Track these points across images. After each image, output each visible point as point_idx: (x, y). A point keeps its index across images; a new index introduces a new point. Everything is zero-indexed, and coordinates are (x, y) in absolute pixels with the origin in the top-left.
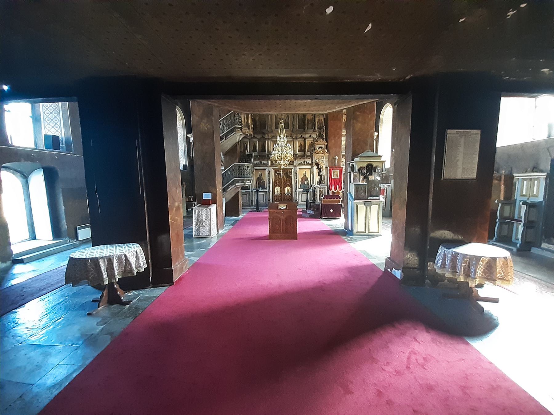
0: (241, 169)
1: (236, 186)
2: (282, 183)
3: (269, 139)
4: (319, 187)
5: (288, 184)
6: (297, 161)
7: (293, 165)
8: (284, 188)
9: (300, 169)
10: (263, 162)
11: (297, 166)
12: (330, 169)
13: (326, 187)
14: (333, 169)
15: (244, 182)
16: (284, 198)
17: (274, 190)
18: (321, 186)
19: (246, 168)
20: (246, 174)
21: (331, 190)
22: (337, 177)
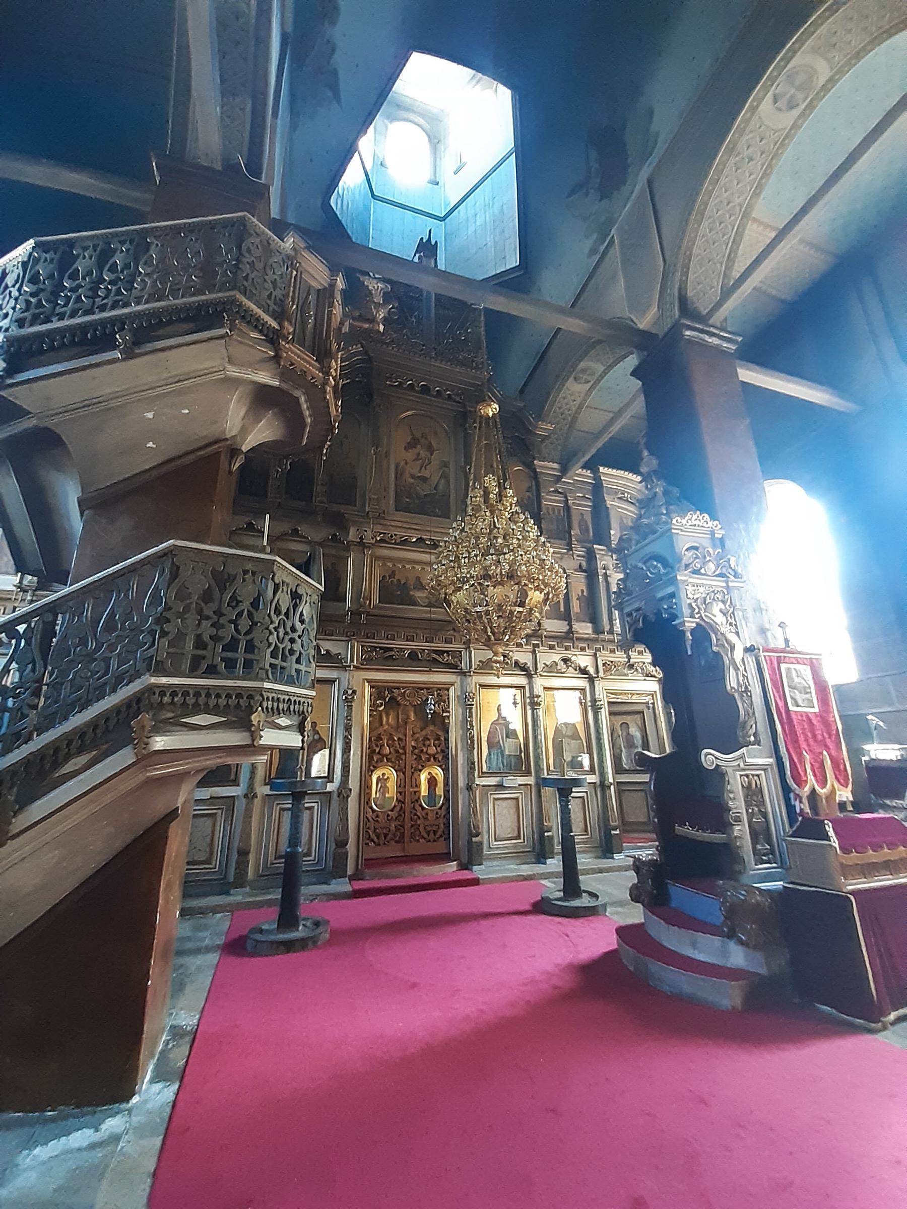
0: (235, 601)
1: (148, 758)
2: (404, 748)
5: (434, 756)
6: (472, 649)
7: (456, 667)
8: (416, 774)
9: (483, 686)
15: (244, 724)
16: (415, 826)
17: (365, 786)
19: (285, 601)
20: (274, 655)
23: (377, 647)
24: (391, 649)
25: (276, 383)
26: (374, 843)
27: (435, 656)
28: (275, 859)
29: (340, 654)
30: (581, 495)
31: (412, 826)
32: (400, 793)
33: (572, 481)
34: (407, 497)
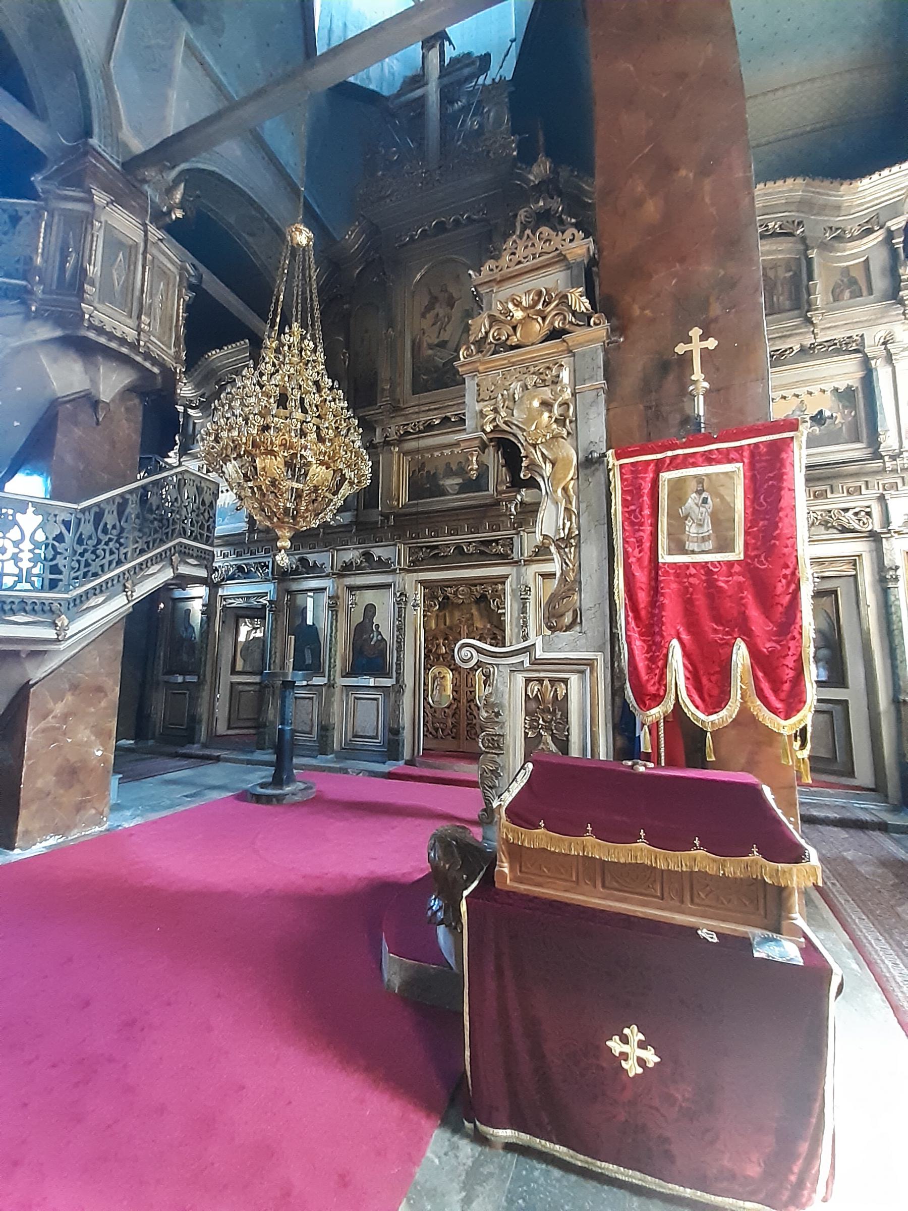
3: (387, 443)
4: (525, 659)
10: (378, 552)
11: (528, 562)
12: (632, 476)
13: (590, 663)
14: (660, 466)
18: (539, 653)
21: (658, 699)
22: (725, 545)
23: (422, 547)
24: (436, 547)
26: (433, 735)
27: (482, 548)
28: (353, 737)
29: (390, 559)
31: (468, 724)
32: (456, 692)
34: (424, 375)
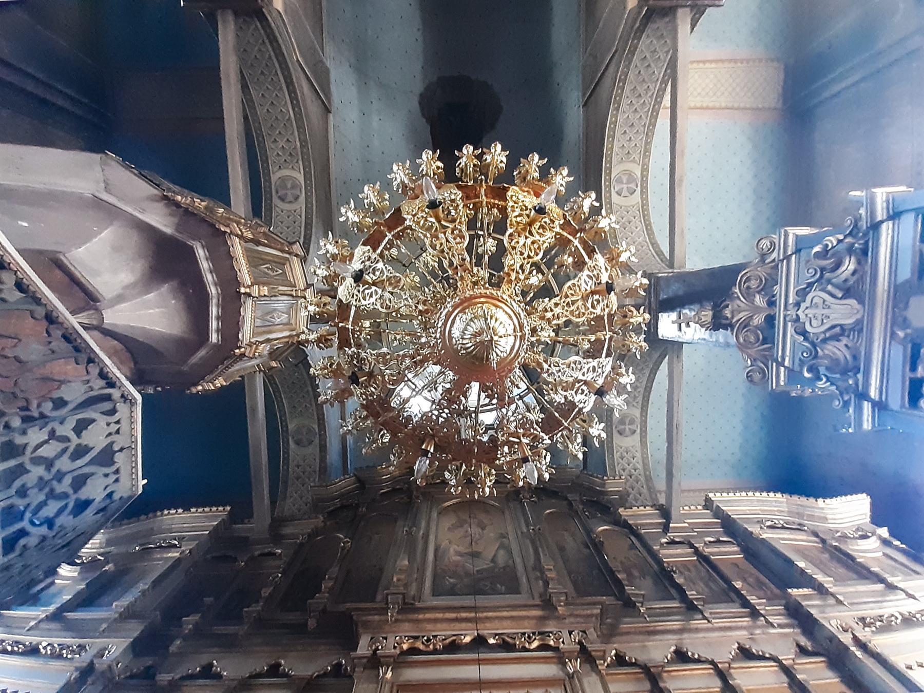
25: (168, 230)
30: (712, 540)
33: (686, 525)
34: (450, 577)
